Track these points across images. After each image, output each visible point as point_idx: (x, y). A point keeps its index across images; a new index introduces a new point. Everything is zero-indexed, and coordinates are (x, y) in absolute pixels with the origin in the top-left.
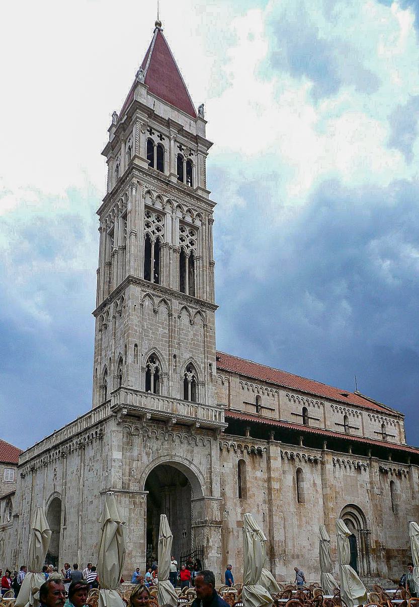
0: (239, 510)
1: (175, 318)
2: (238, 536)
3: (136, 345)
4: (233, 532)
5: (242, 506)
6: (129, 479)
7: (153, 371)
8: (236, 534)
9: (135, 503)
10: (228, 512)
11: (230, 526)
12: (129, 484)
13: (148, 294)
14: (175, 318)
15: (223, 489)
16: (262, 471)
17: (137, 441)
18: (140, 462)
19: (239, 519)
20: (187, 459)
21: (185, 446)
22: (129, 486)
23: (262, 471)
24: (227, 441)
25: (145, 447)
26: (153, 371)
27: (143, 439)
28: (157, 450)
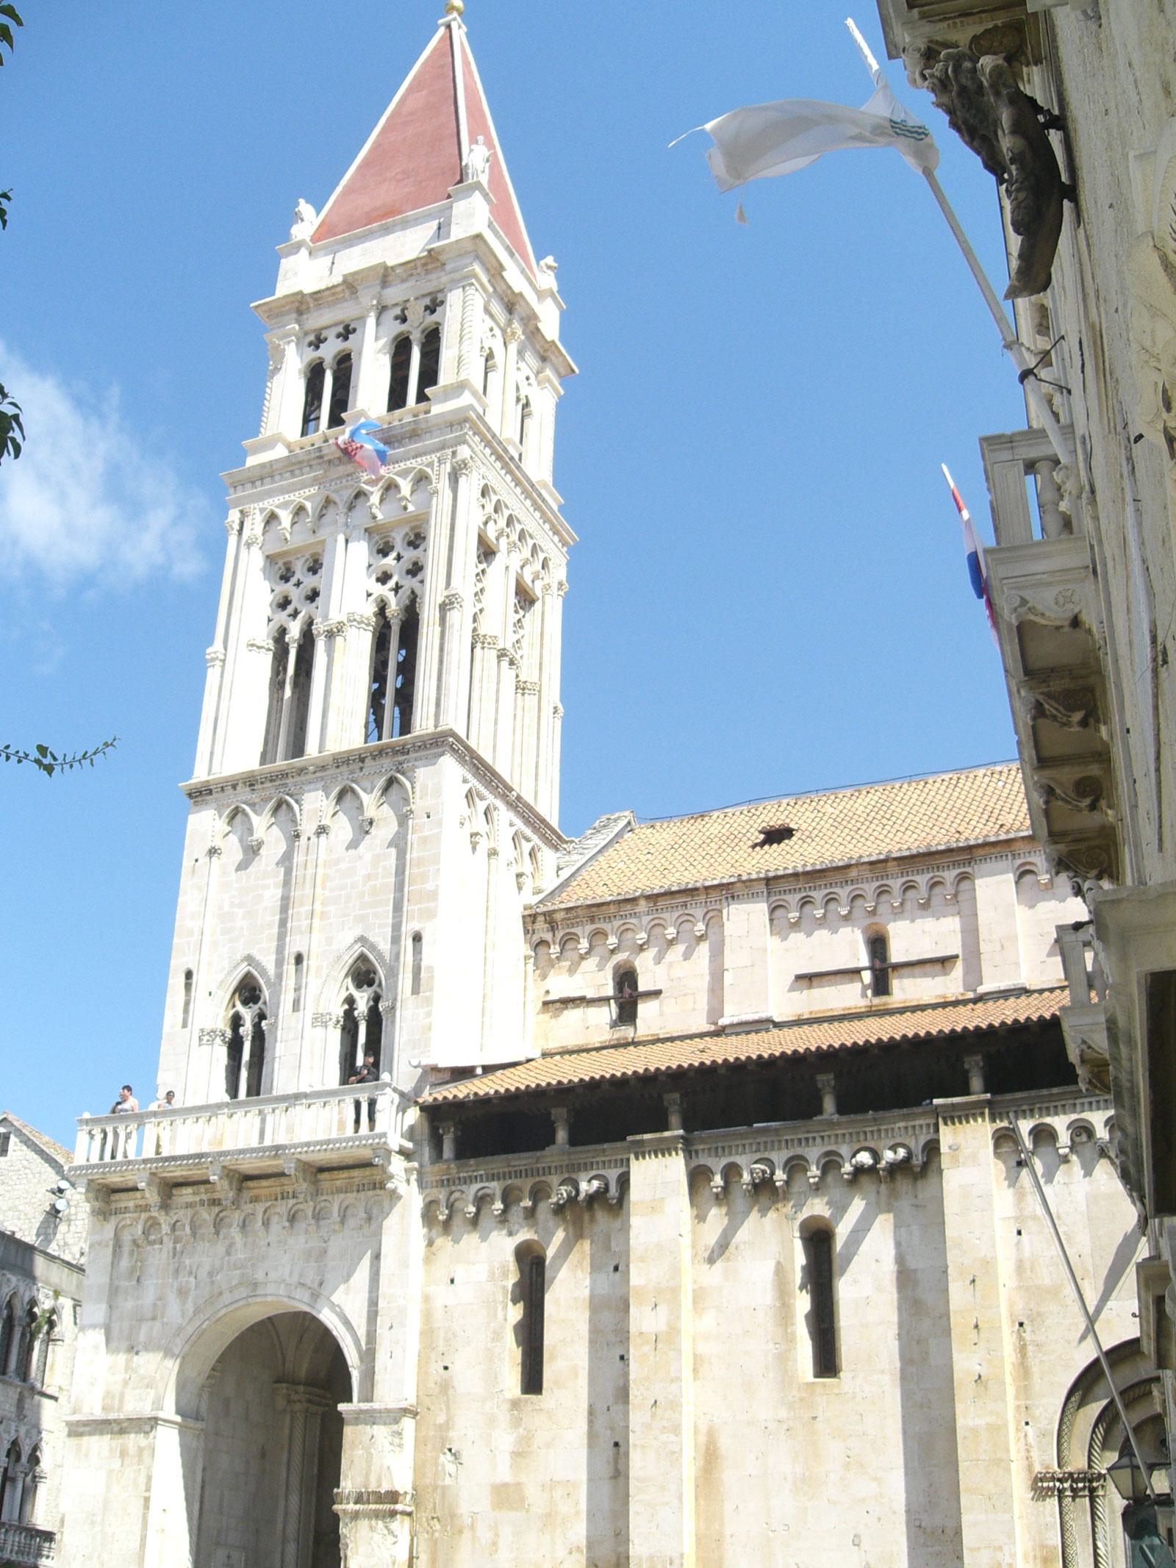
0: (505, 1440)
1: (309, 839)
2: (494, 1544)
3: (189, 975)
4: (472, 1527)
5: (517, 1423)
6: (124, 1380)
7: (247, 1030)
8: (484, 1534)
9: (123, 1454)
10: (456, 1456)
11: (464, 1509)
12: (122, 1395)
13: (237, 808)
14: (309, 839)
15: (446, 1368)
16: (616, 1269)
17: (158, 1257)
18: (157, 1324)
19: (504, 1473)
20: (303, 1285)
21: (300, 1241)
22: (121, 1401)
23: (616, 1269)
24: (464, 1187)
25: (177, 1271)
26: (247, 1030)
27: (175, 1248)
28: (210, 1274)
